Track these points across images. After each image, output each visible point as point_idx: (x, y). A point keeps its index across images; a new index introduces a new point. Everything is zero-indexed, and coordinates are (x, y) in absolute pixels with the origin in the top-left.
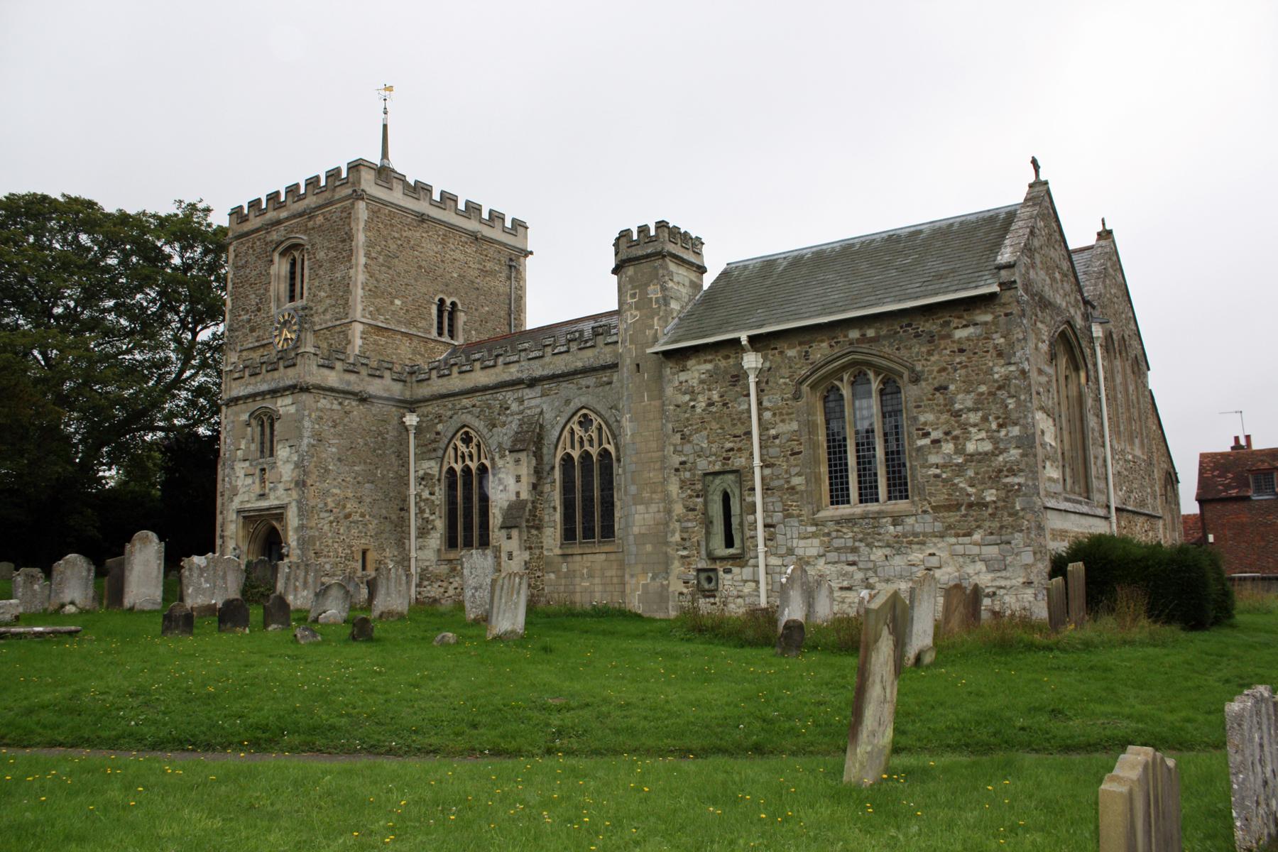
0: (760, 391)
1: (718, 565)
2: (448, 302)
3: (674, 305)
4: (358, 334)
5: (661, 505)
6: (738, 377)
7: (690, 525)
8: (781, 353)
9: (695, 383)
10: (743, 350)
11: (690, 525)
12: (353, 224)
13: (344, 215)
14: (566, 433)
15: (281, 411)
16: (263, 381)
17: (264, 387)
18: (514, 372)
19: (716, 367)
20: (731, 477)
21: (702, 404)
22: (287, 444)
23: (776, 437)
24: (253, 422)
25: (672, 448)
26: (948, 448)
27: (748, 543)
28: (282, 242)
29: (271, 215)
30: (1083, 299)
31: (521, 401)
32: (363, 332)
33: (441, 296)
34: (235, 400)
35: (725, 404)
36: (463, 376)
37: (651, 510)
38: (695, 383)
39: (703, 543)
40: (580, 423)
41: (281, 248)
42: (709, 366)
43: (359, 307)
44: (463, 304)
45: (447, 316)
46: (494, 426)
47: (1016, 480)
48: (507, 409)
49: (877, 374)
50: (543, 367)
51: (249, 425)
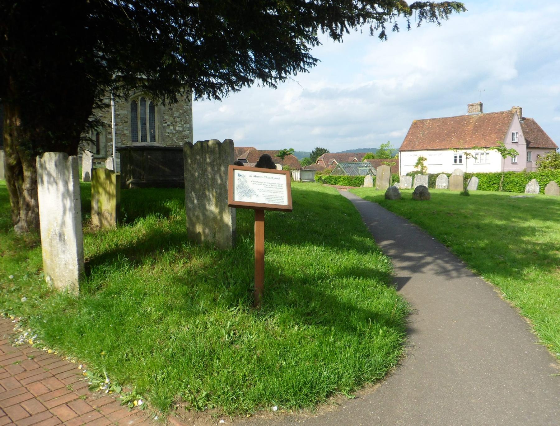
27: (108, 153)
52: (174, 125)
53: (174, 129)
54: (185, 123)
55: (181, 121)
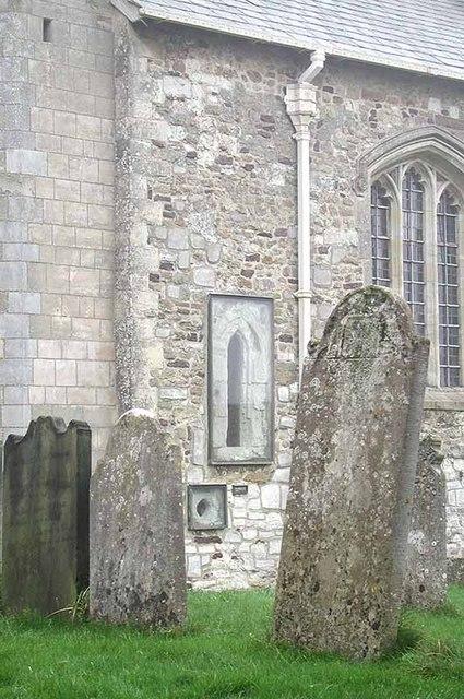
1: (226, 479)
5: (94, 347)
7: (175, 394)
8: (338, 100)
9: (197, 106)
11: (175, 394)
19: (239, 88)
20: (254, 309)
21: (206, 158)
25: (144, 231)
37: (69, 354)
38: (197, 106)
39: (201, 434)
42: (226, 84)
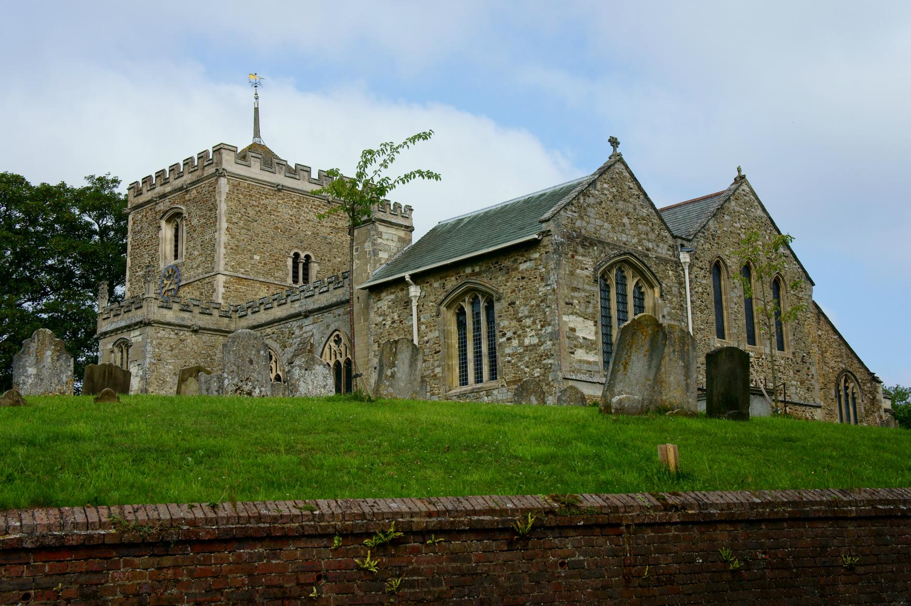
0: (419, 311)
2: (302, 255)
3: (383, 255)
4: (221, 284)
6: (408, 303)
10: (408, 285)
12: (217, 197)
13: (211, 189)
14: (327, 349)
15: (133, 340)
16: (122, 319)
17: (123, 324)
18: (296, 308)
19: (397, 297)
22: (136, 363)
23: (427, 342)
24: (116, 350)
26: (515, 342)
28: (167, 211)
29: (159, 190)
30: (672, 235)
31: (301, 327)
32: (226, 282)
33: (296, 251)
34: (105, 334)
35: (401, 322)
36: (267, 312)
40: (335, 341)
41: (166, 217)
42: (393, 297)
43: (222, 263)
44: (316, 257)
45: (301, 267)
46: (285, 347)
47: (550, 361)
48: (293, 334)
49: (483, 296)
50: (314, 302)
51: (112, 352)
52: (519, 336)
53: (521, 344)
54: (542, 326)
55: (534, 323)
